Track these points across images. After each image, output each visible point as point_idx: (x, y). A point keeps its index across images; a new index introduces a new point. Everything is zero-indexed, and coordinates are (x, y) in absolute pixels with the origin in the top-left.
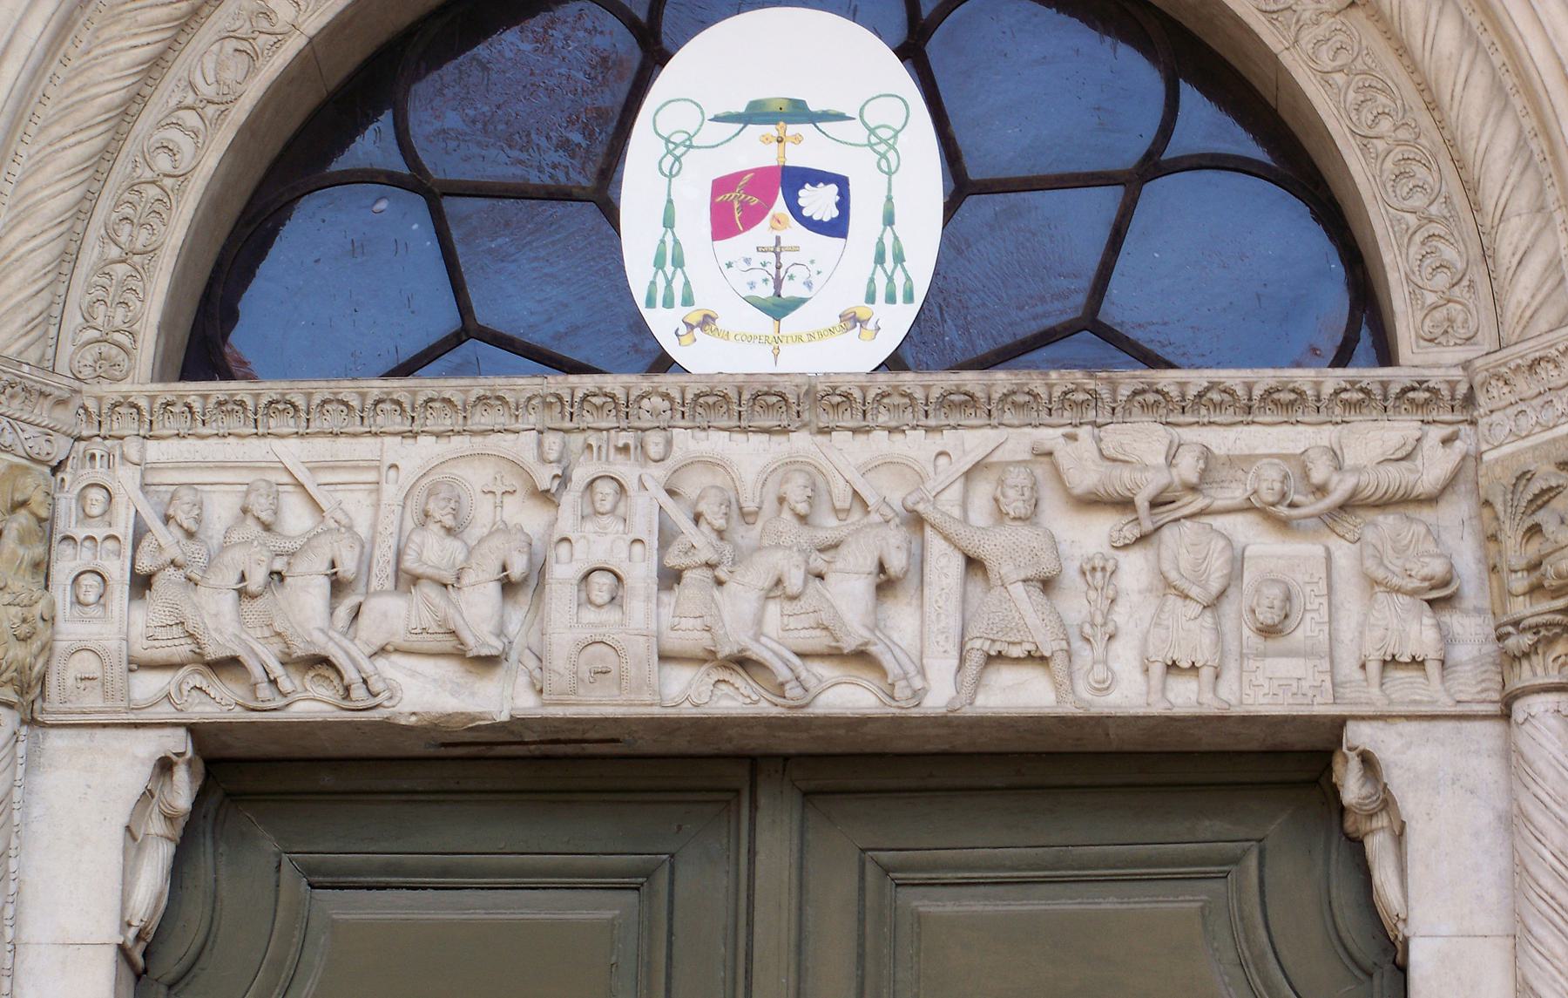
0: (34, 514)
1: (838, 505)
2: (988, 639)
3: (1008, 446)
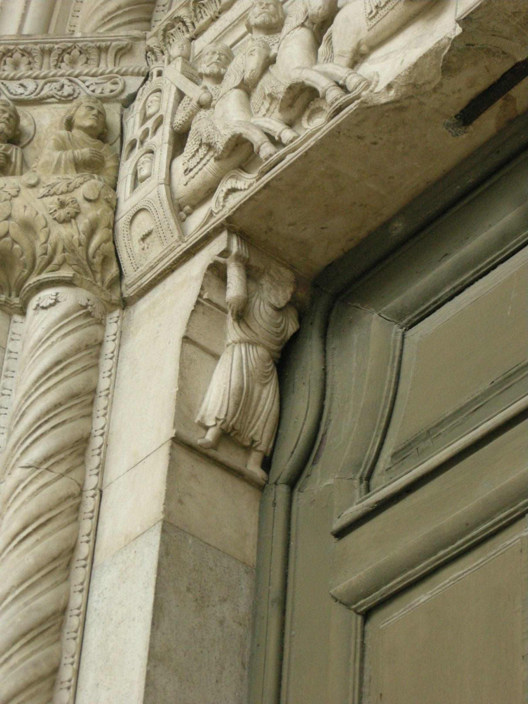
0: (80, 128)
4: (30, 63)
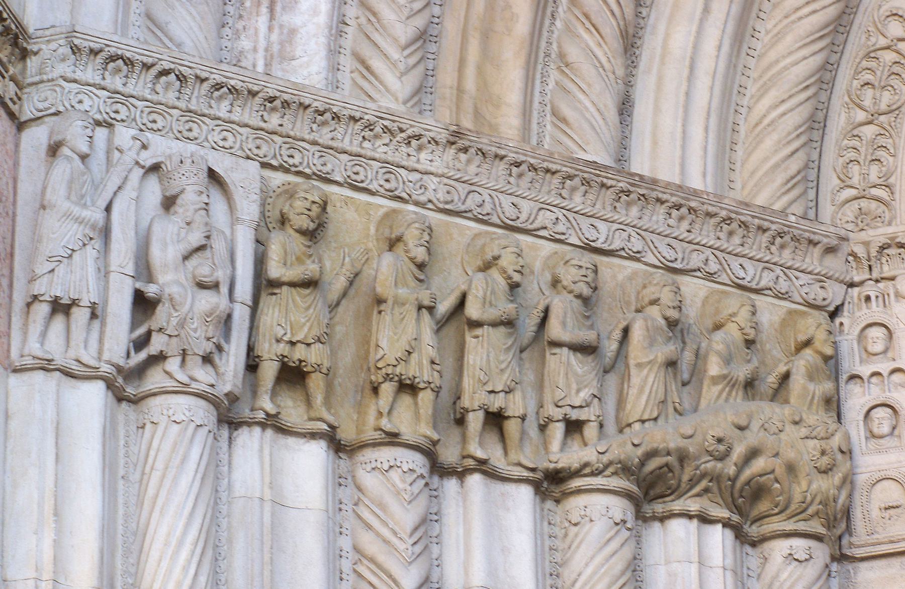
4: (744, 236)
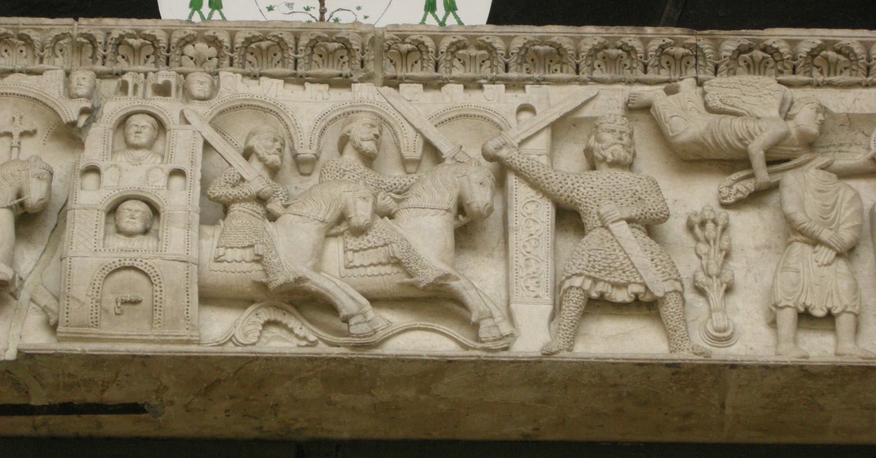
1: (408, 155)
2: (589, 277)
3: (598, 103)
